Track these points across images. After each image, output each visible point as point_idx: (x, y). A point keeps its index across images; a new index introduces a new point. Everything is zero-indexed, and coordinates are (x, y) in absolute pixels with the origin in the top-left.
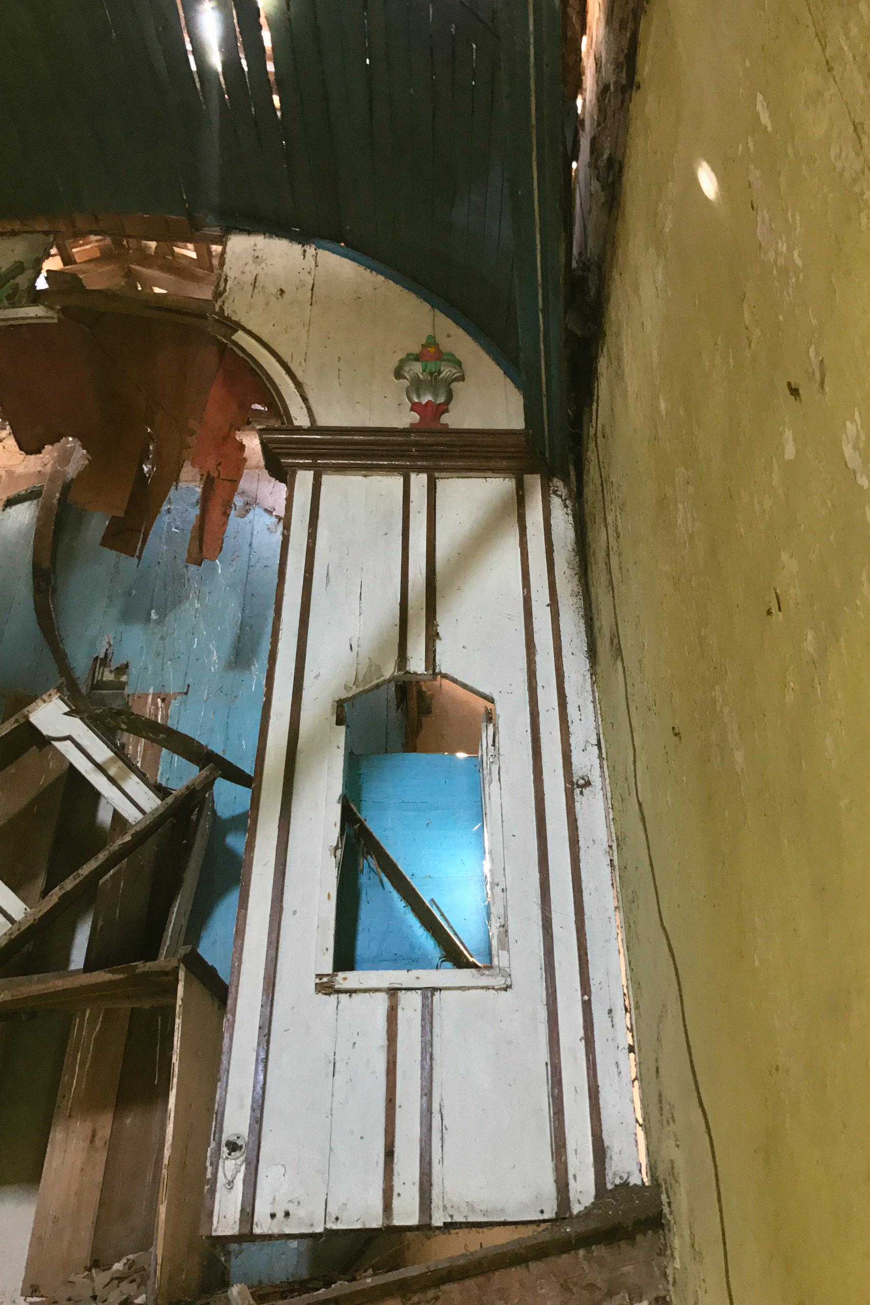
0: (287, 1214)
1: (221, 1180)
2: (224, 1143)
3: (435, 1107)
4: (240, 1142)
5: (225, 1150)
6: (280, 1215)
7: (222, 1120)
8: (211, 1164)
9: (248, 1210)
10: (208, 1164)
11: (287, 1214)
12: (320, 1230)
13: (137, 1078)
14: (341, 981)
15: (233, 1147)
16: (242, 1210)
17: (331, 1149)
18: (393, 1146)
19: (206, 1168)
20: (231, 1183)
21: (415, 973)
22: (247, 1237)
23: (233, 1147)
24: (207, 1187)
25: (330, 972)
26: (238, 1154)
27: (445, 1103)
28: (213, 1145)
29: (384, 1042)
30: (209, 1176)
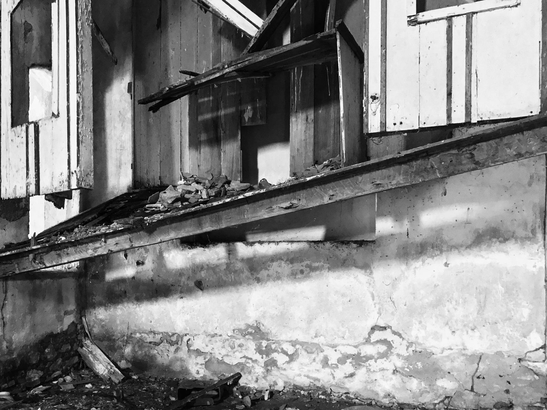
0: (401, 123)
1: (370, 112)
2: (369, 97)
3: (473, 71)
4: (377, 96)
5: (370, 100)
6: (398, 124)
7: (368, 88)
8: (365, 106)
9: (384, 122)
10: (364, 106)
11: (401, 123)
12: (417, 128)
13: (322, 94)
14: (421, 17)
15: (374, 98)
16: (381, 122)
17: (420, 95)
18: (451, 91)
19: (363, 108)
20: (375, 114)
21: (462, 6)
22: (383, 133)
23: (374, 98)
24: (364, 115)
25: (415, 14)
26: (376, 101)
27: (478, 69)
28: (365, 98)
29: (445, 44)
30: (364, 110)
